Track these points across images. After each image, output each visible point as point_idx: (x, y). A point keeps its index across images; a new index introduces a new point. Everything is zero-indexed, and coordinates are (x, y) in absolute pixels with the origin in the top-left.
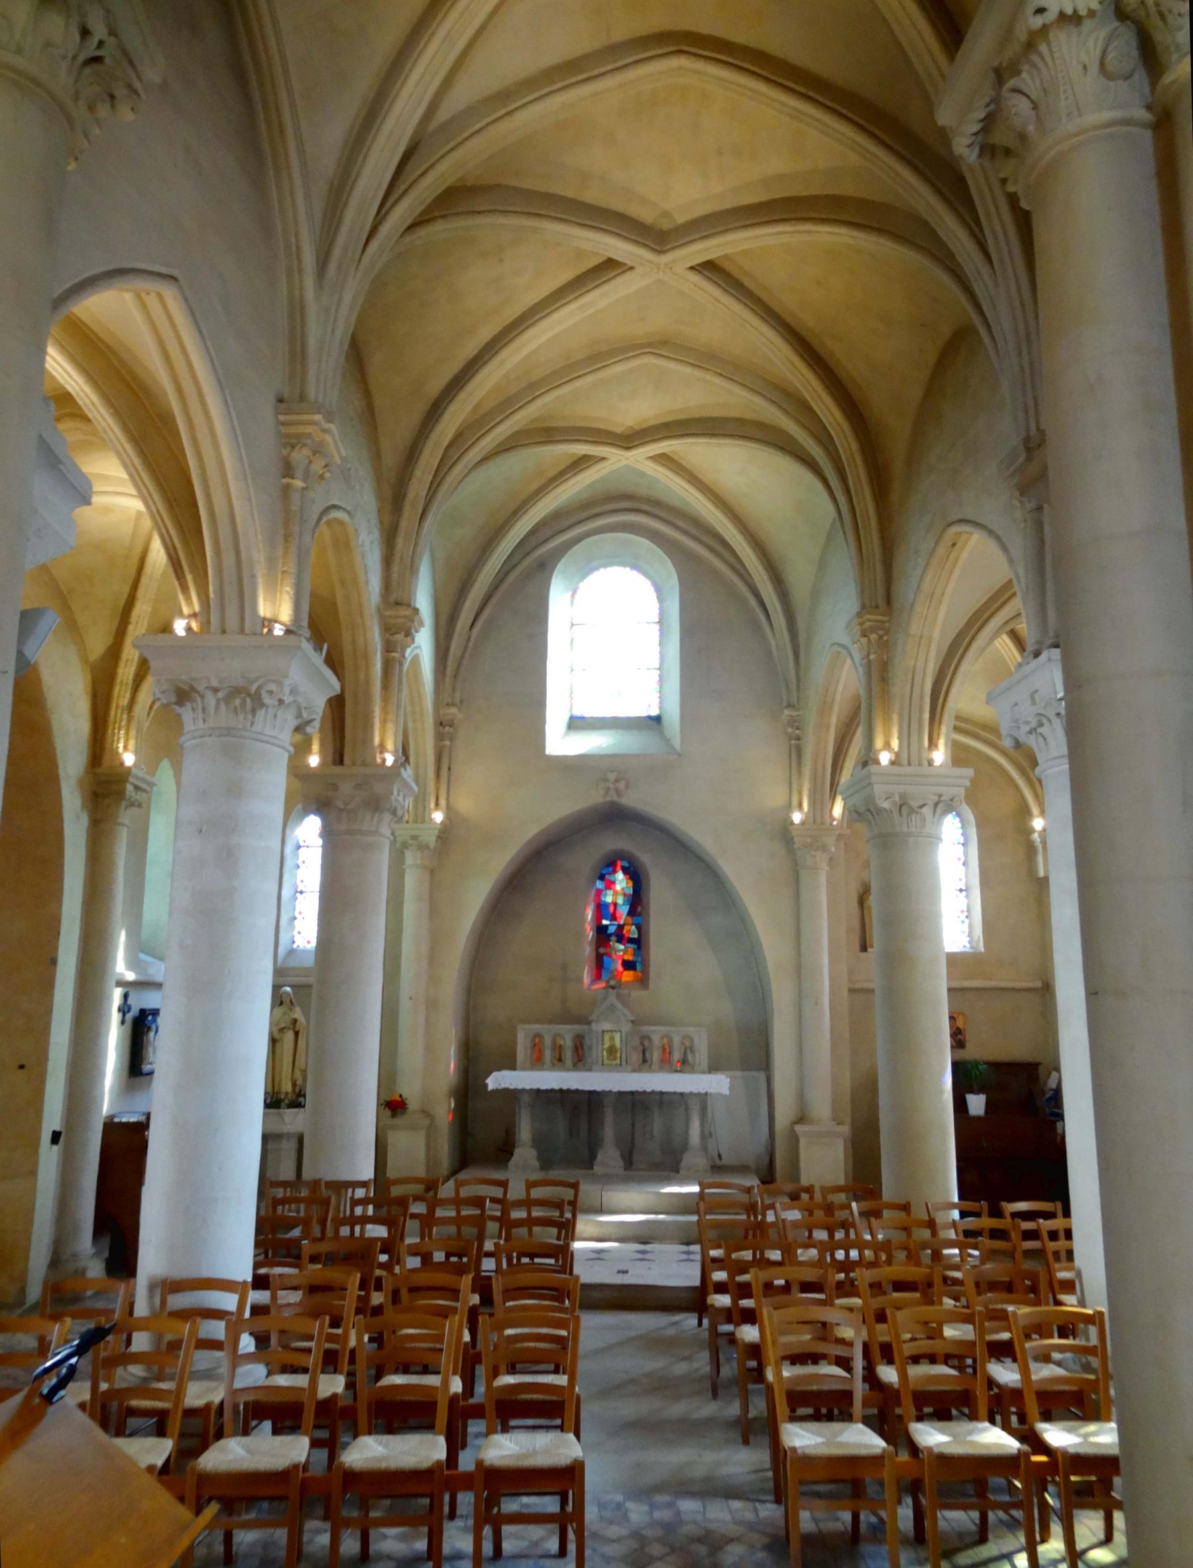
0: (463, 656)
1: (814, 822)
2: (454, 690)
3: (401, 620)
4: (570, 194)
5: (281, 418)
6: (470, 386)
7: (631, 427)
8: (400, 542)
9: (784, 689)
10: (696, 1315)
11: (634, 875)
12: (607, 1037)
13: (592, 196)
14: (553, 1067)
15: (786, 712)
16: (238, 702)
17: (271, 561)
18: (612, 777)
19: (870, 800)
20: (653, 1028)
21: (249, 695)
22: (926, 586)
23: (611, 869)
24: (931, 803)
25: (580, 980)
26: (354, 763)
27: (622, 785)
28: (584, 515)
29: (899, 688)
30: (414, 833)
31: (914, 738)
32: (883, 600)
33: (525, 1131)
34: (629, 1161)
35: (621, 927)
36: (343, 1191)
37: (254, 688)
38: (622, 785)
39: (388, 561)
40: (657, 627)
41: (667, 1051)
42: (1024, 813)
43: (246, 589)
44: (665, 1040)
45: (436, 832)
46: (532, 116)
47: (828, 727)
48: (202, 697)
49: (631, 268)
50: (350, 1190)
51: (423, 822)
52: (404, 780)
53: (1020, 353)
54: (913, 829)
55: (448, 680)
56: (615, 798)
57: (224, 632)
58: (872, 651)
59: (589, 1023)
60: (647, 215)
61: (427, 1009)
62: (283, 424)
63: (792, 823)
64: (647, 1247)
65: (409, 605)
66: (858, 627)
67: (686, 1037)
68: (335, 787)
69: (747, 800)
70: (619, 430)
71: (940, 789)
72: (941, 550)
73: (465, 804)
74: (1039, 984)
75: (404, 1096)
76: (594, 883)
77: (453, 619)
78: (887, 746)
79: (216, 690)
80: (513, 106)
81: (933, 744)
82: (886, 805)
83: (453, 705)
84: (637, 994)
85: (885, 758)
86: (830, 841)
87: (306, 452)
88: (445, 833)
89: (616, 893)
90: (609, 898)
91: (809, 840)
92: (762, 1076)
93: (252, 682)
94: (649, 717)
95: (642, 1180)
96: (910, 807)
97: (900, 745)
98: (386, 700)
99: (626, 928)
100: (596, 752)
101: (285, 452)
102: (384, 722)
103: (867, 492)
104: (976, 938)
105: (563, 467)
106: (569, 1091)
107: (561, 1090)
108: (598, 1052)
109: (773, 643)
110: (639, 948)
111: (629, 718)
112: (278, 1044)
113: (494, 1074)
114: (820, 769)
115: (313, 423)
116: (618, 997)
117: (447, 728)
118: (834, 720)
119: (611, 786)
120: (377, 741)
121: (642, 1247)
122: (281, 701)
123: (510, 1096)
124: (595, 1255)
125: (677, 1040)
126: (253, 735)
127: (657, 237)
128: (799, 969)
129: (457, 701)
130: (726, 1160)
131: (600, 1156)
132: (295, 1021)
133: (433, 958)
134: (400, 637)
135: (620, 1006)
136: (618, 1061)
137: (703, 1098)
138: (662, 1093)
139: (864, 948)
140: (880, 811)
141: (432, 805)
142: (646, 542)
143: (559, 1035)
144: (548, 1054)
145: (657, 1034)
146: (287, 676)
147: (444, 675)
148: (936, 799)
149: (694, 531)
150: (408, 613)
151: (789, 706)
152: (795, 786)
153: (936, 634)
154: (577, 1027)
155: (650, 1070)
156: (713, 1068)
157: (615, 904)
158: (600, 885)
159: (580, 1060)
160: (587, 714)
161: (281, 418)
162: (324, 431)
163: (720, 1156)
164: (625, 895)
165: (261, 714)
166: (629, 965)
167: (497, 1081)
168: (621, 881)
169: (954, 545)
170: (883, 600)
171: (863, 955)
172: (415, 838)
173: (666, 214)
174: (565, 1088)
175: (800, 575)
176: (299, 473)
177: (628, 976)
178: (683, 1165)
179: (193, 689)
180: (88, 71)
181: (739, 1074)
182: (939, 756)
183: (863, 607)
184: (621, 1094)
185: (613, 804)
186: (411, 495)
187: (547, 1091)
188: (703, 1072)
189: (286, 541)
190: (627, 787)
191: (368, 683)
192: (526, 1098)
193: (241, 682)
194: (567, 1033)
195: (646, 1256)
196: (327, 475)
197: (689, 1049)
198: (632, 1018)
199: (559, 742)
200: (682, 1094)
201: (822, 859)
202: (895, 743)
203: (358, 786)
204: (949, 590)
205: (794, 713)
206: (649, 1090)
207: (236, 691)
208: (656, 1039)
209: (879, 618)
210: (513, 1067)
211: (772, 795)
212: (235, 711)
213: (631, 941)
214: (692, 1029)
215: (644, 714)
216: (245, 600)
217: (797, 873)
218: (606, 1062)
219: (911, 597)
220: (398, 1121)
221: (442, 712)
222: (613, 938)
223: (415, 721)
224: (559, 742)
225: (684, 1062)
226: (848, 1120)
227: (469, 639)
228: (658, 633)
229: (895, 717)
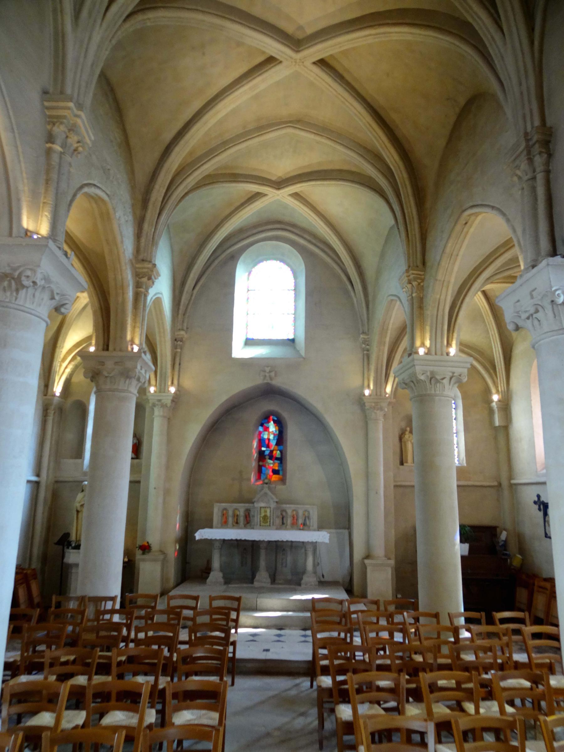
0: (188, 304)
1: (376, 395)
2: (183, 322)
4: (244, 8)
6: (188, 136)
7: (280, 177)
8: (146, 226)
9: (360, 323)
10: (309, 679)
11: (279, 423)
12: (263, 510)
14: (233, 527)
15: (362, 336)
17: (35, 194)
18: (267, 369)
19: (414, 374)
20: (288, 506)
21: (13, 278)
22: (448, 250)
23: (266, 421)
24: (448, 377)
25: (249, 479)
26: (115, 350)
27: (273, 374)
28: (254, 231)
29: (430, 311)
30: (159, 398)
31: (439, 340)
32: (421, 262)
33: (216, 564)
34: (273, 580)
35: (272, 452)
36: (99, 603)
37: (16, 274)
38: (273, 374)
39: (138, 235)
40: (293, 292)
41: (295, 518)
42: (487, 392)
44: (295, 513)
45: (171, 398)
47: (385, 343)
50: (103, 603)
51: (164, 392)
52: (144, 360)
53: (520, 84)
54: (438, 392)
55: (180, 316)
56: (269, 381)
58: (414, 291)
59: (253, 503)
60: (290, 29)
62: (48, 108)
63: (364, 395)
64: (282, 632)
65: (150, 262)
66: (406, 278)
67: (306, 511)
68: (103, 363)
69: (342, 382)
70: (274, 179)
71: (454, 369)
72: (458, 227)
73: (188, 383)
74: (495, 483)
75: (150, 543)
76: (258, 428)
77: (183, 284)
78: (423, 345)
81: (449, 344)
82: (422, 378)
83: (183, 330)
84: (280, 487)
85: (422, 351)
86: (384, 405)
87: (62, 128)
88: (176, 399)
89: (269, 435)
90: (266, 437)
91: (373, 404)
92: (346, 532)
94: (288, 340)
95: (279, 591)
96: (436, 379)
97: (431, 344)
98: (135, 315)
99: (274, 452)
100: (259, 356)
101: (49, 127)
102: (134, 327)
103: (411, 199)
104: (461, 458)
105: (243, 200)
106: (241, 540)
107: (236, 540)
108: (257, 519)
109: (355, 300)
110: (281, 463)
111: (277, 340)
112: (80, 515)
113: (200, 531)
114: (379, 367)
115: (69, 108)
116: (269, 488)
117: (179, 342)
118: (388, 339)
119: (267, 375)
120: (129, 337)
121: (278, 632)
122: (34, 283)
123: (209, 542)
124: (251, 638)
125: (301, 513)
126: (16, 306)
127: (296, 43)
128: (368, 475)
129: (185, 328)
130: (327, 579)
131: (257, 577)
133: (168, 466)
134: (145, 280)
135: (270, 493)
136: (268, 524)
137: (314, 545)
138: (292, 542)
139: (402, 463)
140: (419, 381)
141: (170, 383)
142: (288, 246)
143: (236, 509)
144: (230, 520)
145: (289, 509)
146: (39, 266)
147: (178, 315)
148: (451, 374)
149: (314, 241)
150: (150, 266)
151: (363, 333)
152: (366, 376)
153: (453, 280)
154: (247, 505)
155: (286, 529)
156: (320, 528)
157: (269, 439)
158: (261, 429)
159: (248, 523)
160: (255, 337)
161: (46, 104)
163: (323, 576)
164: (274, 434)
165: (22, 293)
166: (275, 472)
167: (201, 534)
168: (272, 427)
169: (466, 223)
170: (421, 262)
171: (401, 467)
172: (160, 401)
173: (300, 28)
174: (239, 538)
175: (370, 263)
176: (59, 141)
177: (275, 478)
178: (303, 582)
181: (333, 531)
182: (453, 351)
183: (409, 267)
184: (269, 542)
185: (268, 384)
186: (153, 199)
187: (228, 540)
188: (314, 530)
189: (47, 183)
190: (276, 375)
191: (124, 303)
192: (217, 545)
193: (8, 270)
194: (241, 508)
195: (281, 639)
196: (80, 149)
197: (307, 517)
198: (277, 500)
199: (239, 351)
200: (303, 542)
201: (380, 414)
202: (428, 343)
204: (461, 253)
205: (366, 337)
206: (285, 540)
208: (289, 512)
209: (419, 273)
210: (211, 527)
211: (353, 380)
212: (4, 290)
213: (277, 459)
214: (308, 506)
215: (286, 338)
217: (366, 423)
218: (262, 524)
219: (438, 258)
220: (146, 557)
221: (176, 333)
222: (267, 457)
223: (160, 337)
224: (239, 351)
225: (304, 524)
226: (393, 556)
227: (192, 296)
228: (294, 295)
229: (428, 328)
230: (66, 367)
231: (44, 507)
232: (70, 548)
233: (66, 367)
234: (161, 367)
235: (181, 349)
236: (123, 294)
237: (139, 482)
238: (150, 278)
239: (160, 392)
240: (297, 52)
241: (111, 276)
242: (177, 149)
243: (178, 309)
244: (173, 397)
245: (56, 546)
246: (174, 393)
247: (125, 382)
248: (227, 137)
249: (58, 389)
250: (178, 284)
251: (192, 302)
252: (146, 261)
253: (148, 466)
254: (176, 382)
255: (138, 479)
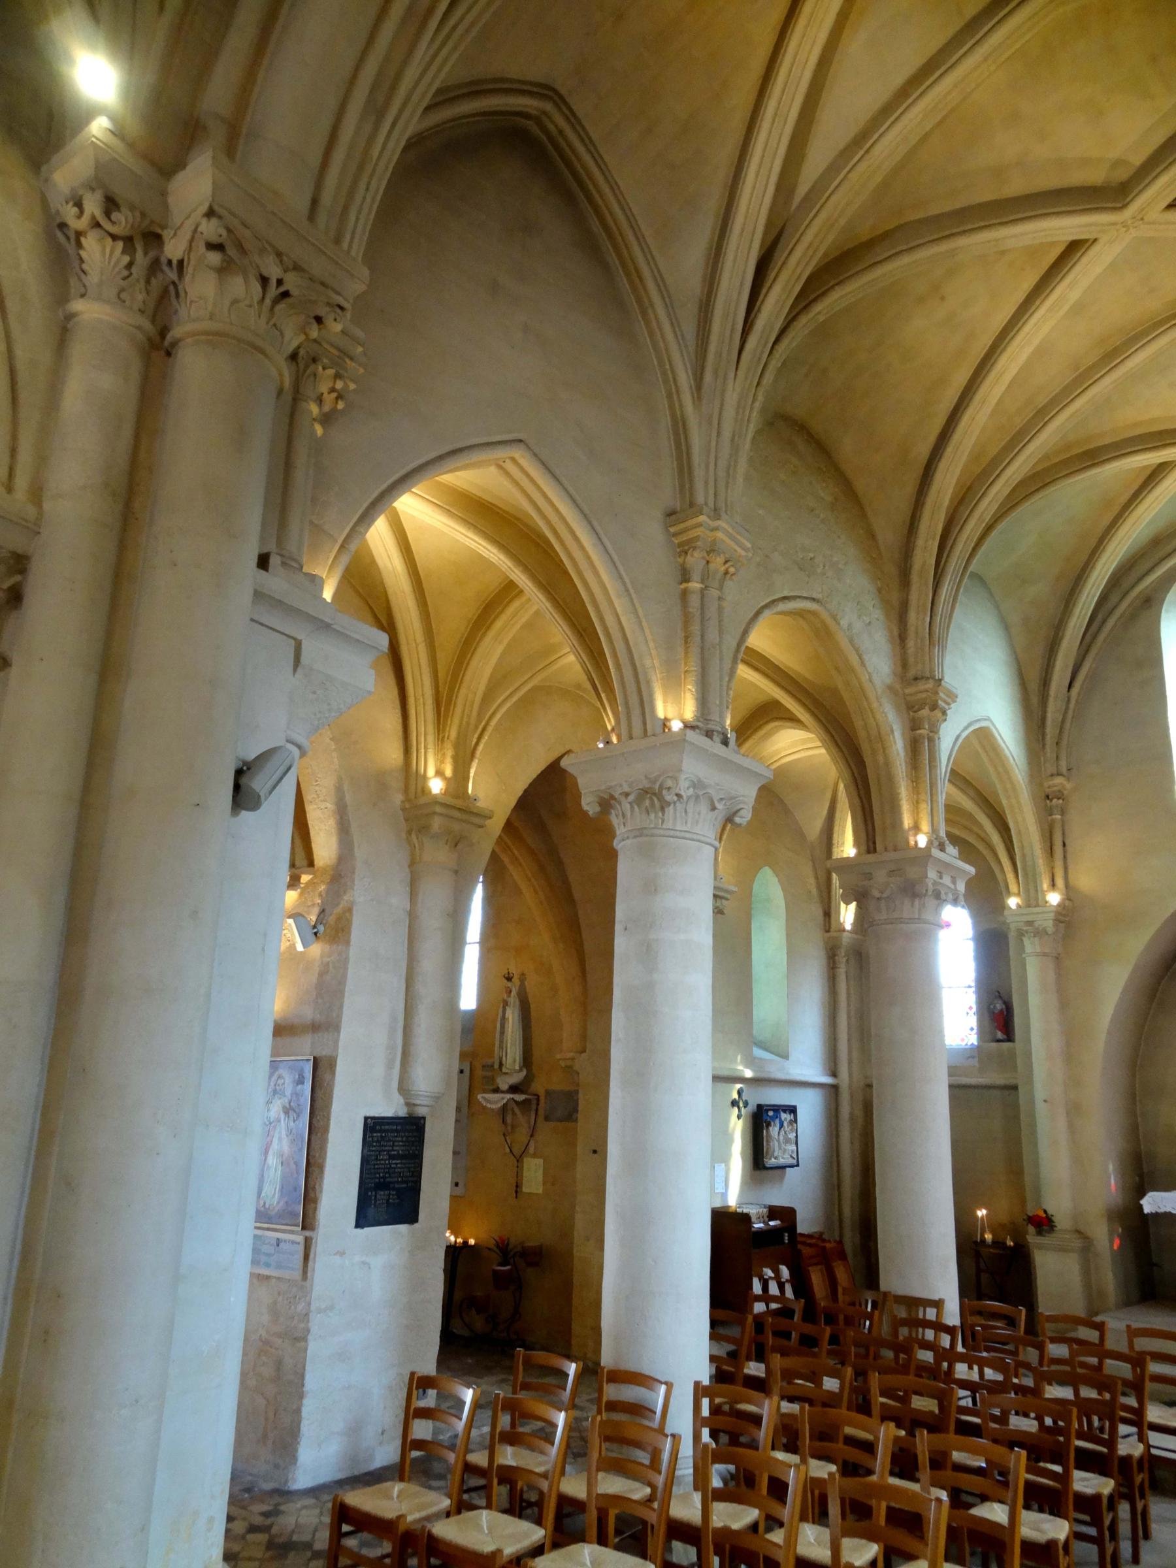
0: (1063, 721)
3: (924, 695)
5: (672, 530)
6: (956, 437)
8: (912, 616)
13: (1016, 186)
16: (647, 802)
21: (655, 794)
30: (1029, 918)
43: (645, 694)
45: (1052, 915)
46: (889, 146)
48: (620, 804)
49: (1095, 240)
50: (921, 1309)
51: (1037, 906)
55: (1048, 749)
57: (631, 738)
60: (1095, 176)
61: (1068, 1114)
62: (675, 535)
65: (933, 677)
68: (869, 876)
73: (1087, 880)
75: (1050, 1213)
77: (1045, 683)
79: (627, 795)
80: (868, 145)
87: (697, 554)
88: (1066, 917)
93: (654, 782)
101: (680, 560)
102: (916, 805)
105: (1136, 486)
113: (1151, 1194)
115: (700, 525)
117: (1055, 801)
120: (907, 822)
126: (662, 832)
127: (1113, 194)
129: (1064, 770)
134: (925, 712)
141: (1045, 886)
146: (681, 770)
150: (930, 685)
161: (672, 530)
162: (716, 529)
172: (1030, 923)
173: (1118, 163)
176: (696, 576)
179: (612, 797)
180: (281, 306)
189: (686, 642)
193: (645, 784)
196: (732, 570)
203: (891, 873)
207: (645, 792)
212: (648, 813)
216: (645, 704)
221: (1046, 784)
223: (1008, 798)
231: (852, 1133)
234: (1024, 856)
235: (1063, 813)
236: (884, 749)
237: (1014, 1088)
238: (934, 707)
239: (1028, 906)
240: (1125, 206)
241: (858, 723)
242: (943, 465)
243: (1044, 735)
244: (1058, 913)
246: (1059, 905)
247: (912, 905)
248: (1042, 401)
250: (1034, 686)
251: (1070, 713)
252: (922, 678)
253: (1028, 1054)
254: (1060, 882)
255: (1011, 1082)
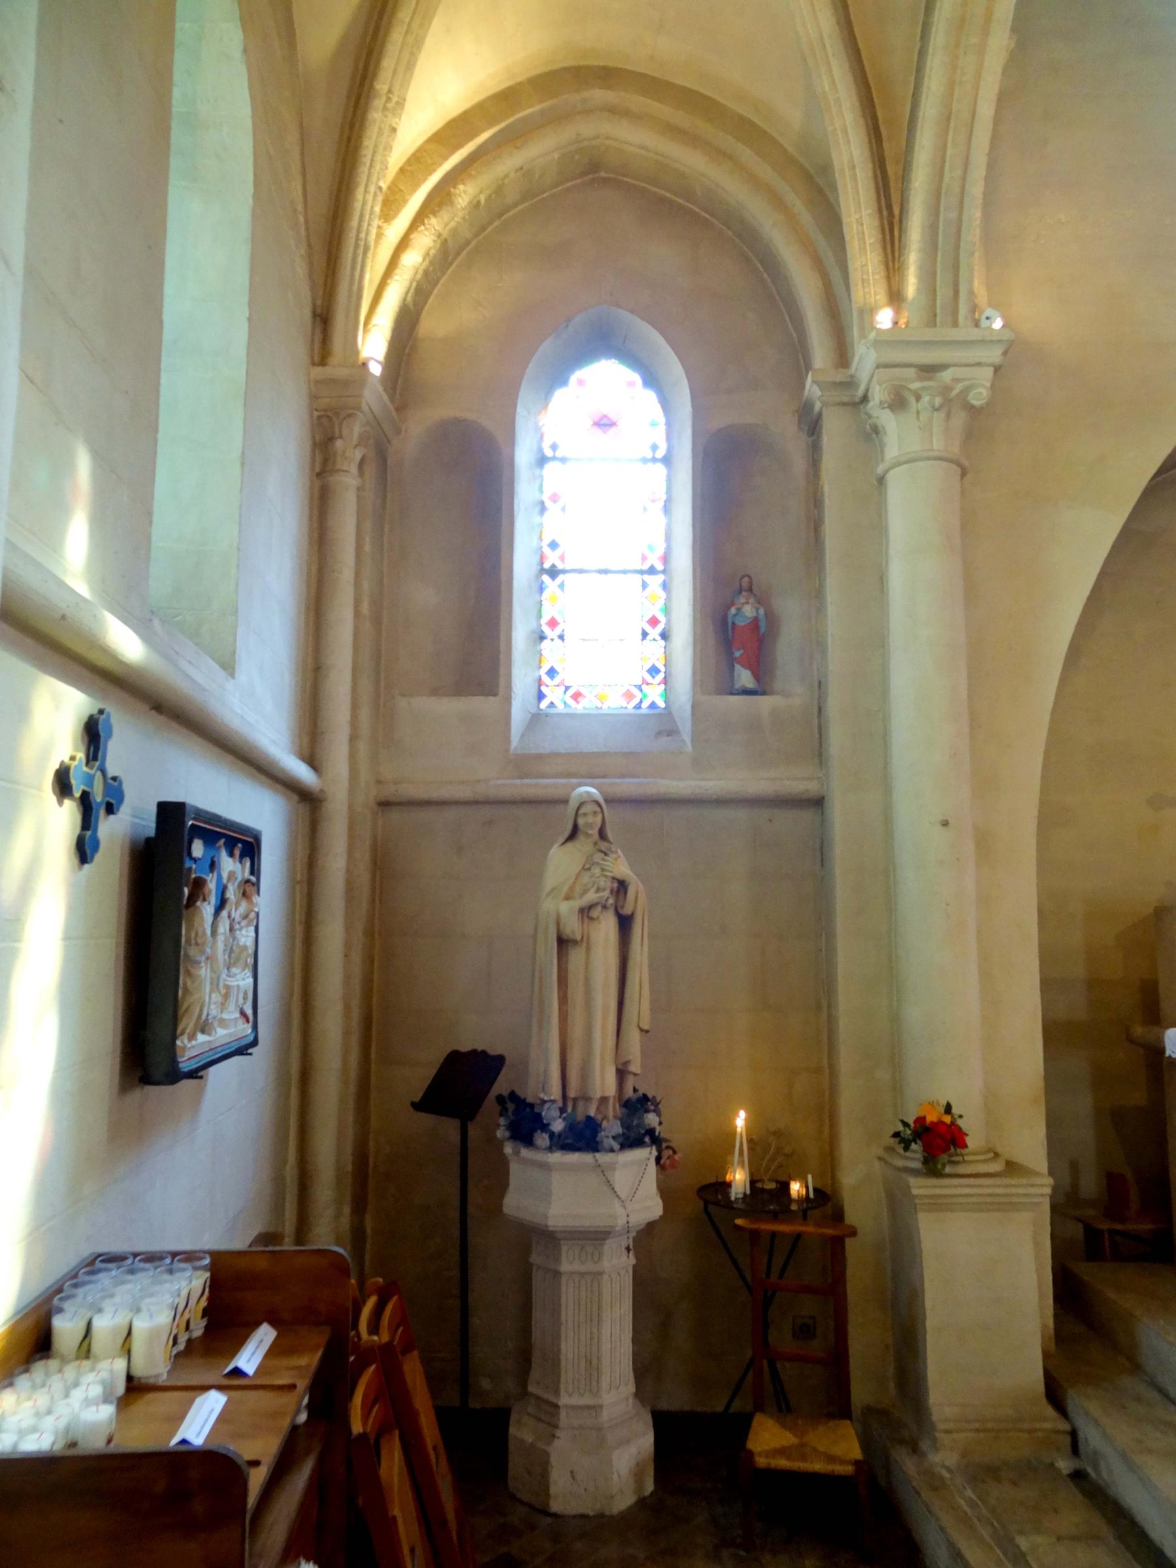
45: (994, 355)
112: (576, 957)
132: (622, 886)
133: (979, 720)
172: (929, 370)
230: (403, 244)
231: (348, 927)
232: (542, 1139)
233: (403, 244)
245: (426, 1120)
249: (374, 345)
255: (811, 787)
